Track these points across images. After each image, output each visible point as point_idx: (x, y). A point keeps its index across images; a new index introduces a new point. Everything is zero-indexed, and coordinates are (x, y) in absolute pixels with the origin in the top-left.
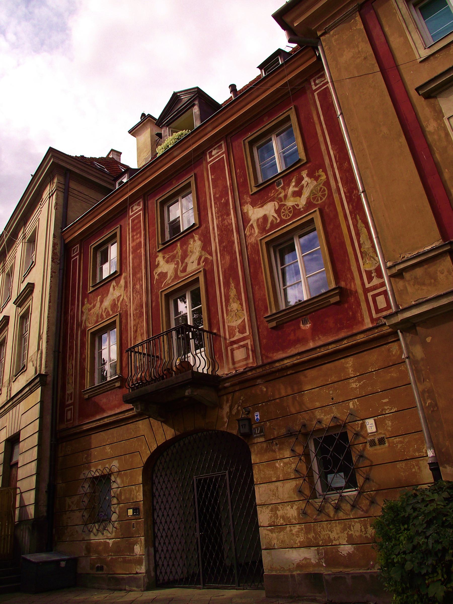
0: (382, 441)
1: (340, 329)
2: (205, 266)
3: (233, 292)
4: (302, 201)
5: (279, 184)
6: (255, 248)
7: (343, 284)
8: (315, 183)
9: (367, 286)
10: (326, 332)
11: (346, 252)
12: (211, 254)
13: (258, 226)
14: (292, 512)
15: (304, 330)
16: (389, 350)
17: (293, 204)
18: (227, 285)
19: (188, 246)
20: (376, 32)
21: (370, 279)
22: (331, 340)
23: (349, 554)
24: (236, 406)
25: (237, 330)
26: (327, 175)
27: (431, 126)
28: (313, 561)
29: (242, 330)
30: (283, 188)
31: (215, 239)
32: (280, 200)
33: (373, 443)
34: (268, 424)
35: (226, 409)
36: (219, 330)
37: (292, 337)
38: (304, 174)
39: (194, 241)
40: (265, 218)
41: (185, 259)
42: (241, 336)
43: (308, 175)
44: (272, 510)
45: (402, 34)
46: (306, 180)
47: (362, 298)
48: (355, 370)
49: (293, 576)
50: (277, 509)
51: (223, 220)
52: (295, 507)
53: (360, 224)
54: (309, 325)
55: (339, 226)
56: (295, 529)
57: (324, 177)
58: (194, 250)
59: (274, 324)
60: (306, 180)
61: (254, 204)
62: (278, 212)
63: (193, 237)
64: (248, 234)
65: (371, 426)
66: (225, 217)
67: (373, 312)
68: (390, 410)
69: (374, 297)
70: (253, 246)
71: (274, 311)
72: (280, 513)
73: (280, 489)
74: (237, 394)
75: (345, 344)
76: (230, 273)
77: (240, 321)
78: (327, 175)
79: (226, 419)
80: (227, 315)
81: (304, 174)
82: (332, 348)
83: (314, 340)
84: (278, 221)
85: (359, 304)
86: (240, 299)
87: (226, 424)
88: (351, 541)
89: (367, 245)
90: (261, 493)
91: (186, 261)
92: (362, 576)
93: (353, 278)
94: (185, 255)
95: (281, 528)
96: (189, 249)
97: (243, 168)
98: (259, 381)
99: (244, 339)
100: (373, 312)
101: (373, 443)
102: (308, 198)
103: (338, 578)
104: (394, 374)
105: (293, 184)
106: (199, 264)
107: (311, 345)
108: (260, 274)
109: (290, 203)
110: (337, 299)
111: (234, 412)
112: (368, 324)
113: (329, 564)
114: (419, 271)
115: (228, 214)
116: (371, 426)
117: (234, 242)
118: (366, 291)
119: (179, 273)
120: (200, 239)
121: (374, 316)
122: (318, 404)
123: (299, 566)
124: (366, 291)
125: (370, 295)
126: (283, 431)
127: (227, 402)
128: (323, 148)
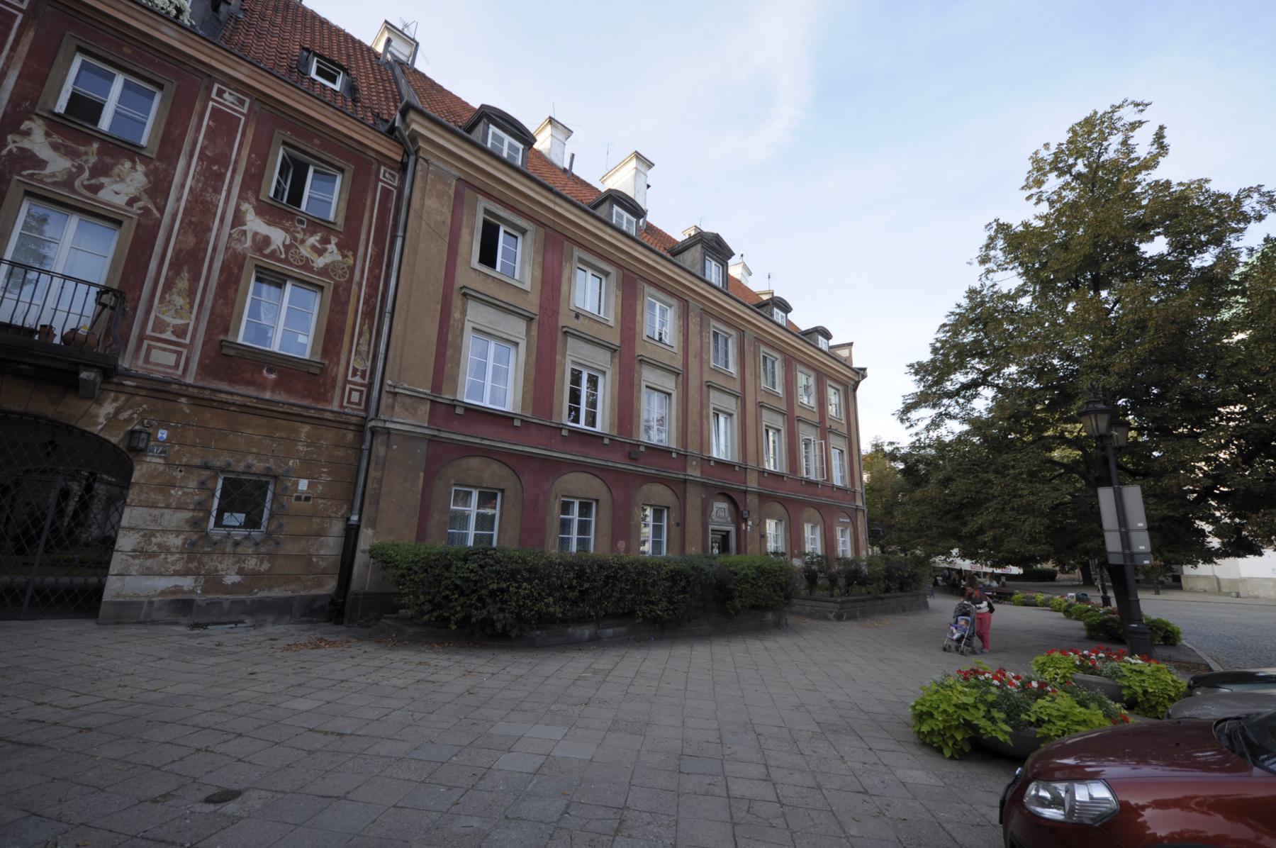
2: (139, 215)
3: (183, 284)
4: (320, 262)
5: (301, 222)
7: (326, 362)
8: (340, 258)
10: (289, 391)
11: (341, 340)
12: (162, 211)
13: (254, 240)
14: (174, 541)
15: (266, 379)
16: (345, 435)
18: (176, 266)
19: (115, 164)
21: (354, 375)
22: (292, 401)
23: (234, 584)
24: (130, 412)
25: (170, 329)
26: (355, 261)
27: (457, 315)
28: (186, 589)
29: (180, 332)
31: (179, 199)
32: (295, 239)
33: (298, 498)
34: (177, 447)
35: (108, 408)
36: (135, 309)
38: (334, 240)
39: (134, 168)
41: (101, 175)
42: (174, 338)
43: (336, 244)
44: (144, 536)
46: (332, 247)
48: (307, 437)
49: (151, 603)
50: (154, 535)
51: (204, 189)
52: (182, 537)
53: (366, 327)
54: (273, 376)
55: (345, 314)
56: (171, 559)
58: (128, 180)
60: (332, 247)
63: (134, 162)
64: (235, 236)
65: (303, 485)
66: (210, 190)
68: (325, 478)
69: (351, 390)
70: (235, 254)
73: (167, 517)
74: (138, 398)
75: (312, 413)
76: (189, 260)
77: (179, 322)
79: (102, 420)
80: (162, 299)
81: (334, 240)
82: (295, 410)
83: (273, 391)
84: (283, 256)
85: (334, 387)
86: (191, 294)
87: (100, 427)
88: (240, 572)
89: (364, 348)
90: (129, 516)
91: (102, 180)
92: (243, 602)
93: (338, 364)
94: (101, 170)
95: (153, 555)
96: (116, 170)
98: (183, 400)
102: (327, 266)
103: (212, 604)
106: (131, 202)
107: (268, 395)
108: (232, 290)
109: (305, 251)
110: (318, 371)
111: (125, 415)
112: (336, 409)
113: (204, 591)
114: (408, 401)
115: (217, 191)
116: (303, 485)
117: (210, 230)
118: (346, 382)
119: (77, 183)
120: (146, 175)
122: (254, 450)
123: (163, 593)
124: (346, 382)
125: (348, 386)
126: (197, 461)
127: (115, 400)
128: (363, 237)
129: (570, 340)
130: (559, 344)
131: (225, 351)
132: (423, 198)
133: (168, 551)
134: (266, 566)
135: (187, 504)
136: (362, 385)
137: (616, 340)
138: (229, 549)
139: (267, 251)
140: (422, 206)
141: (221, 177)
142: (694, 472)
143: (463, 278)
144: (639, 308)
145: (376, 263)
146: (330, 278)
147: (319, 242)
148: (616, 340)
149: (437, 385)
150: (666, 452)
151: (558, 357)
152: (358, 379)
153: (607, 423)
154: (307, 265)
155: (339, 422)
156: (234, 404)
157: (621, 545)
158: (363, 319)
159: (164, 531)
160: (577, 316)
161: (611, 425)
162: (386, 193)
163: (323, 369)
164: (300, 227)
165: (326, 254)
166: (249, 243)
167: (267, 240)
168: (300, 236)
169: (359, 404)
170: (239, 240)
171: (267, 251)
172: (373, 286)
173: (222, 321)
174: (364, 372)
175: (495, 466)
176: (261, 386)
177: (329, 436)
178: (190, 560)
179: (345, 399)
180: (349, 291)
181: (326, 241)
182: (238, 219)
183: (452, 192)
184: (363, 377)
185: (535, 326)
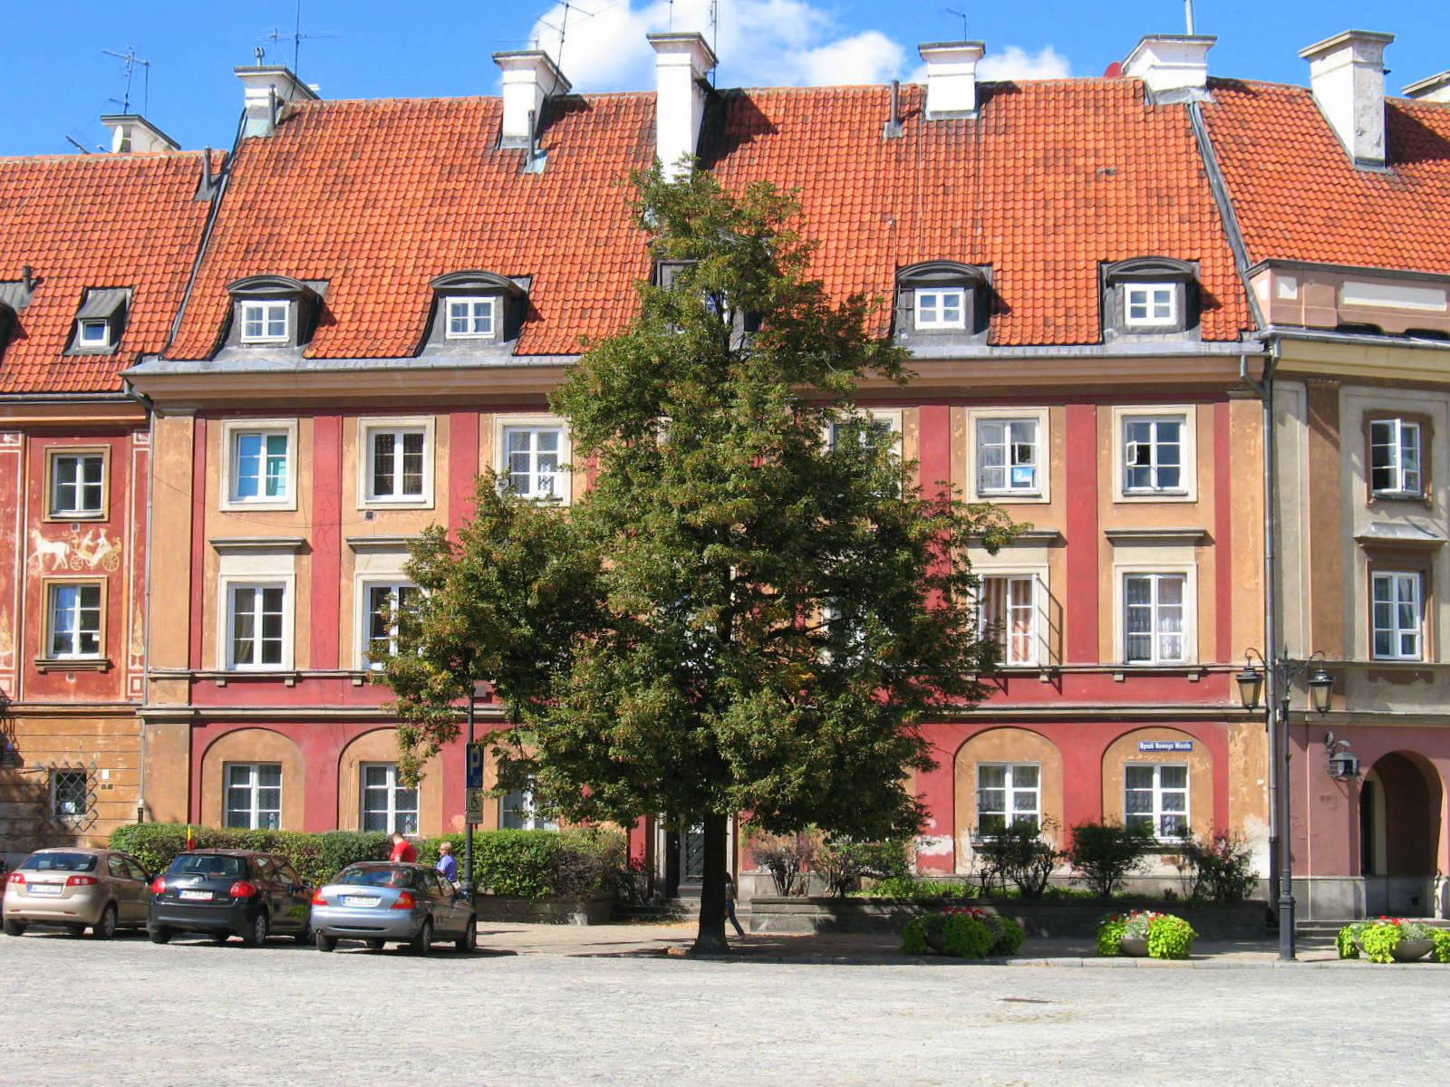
0: (110, 787)
1: (98, 694)
4: (94, 560)
5: (75, 528)
6: (36, 583)
11: (120, 631)
20: (200, 451)
21: (133, 663)
27: (209, 574)
30: (78, 534)
33: (104, 787)
37: (56, 685)
38: (103, 532)
40: (53, 557)
42: (6, 668)
45: (217, 472)
46: (103, 540)
47: (123, 675)
53: (138, 612)
54: (73, 681)
55: (120, 603)
56: (28, 839)
57: (119, 547)
59: (42, 668)
61: (44, 534)
62: (68, 557)
65: (105, 774)
69: (133, 678)
71: (44, 658)
72: (17, 826)
75: (102, 709)
77: (7, 653)
81: (103, 532)
85: (119, 679)
95: (18, 837)
97: (39, 481)
99: (8, 672)
101: (104, 787)
102: (100, 561)
104: (131, 741)
107: (72, 700)
109: (82, 555)
110: (103, 668)
112: (122, 699)
114: (167, 683)
115: (13, 531)
116: (105, 774)
117: (13, 567)
118: (128, 671)
124: (128, 671)
125: (130, 675)
128: (127, 516)
129: (361, 558)
132: (161, 458)
133: (23, 833)
139: (54, 568)
141: (13, 516)
143: (216, 529)
146: (105, 572)
151: (344, 582)
152: (137, 667)
158: (135, 604)
159: (23, 819)
164: (75, 532)
165: (99, 550)
166: (41, 565)
167: (53, 557)
168: (75, 542)
169: (141, 691)
170: (34, 567)
171: (54, 568)
172: (140, 567)
175: (268, 736)
176: (64, 691)
177: (120, 725)
180: (121, 578)
181: (97, 536)
182: (32, 549)
184: (141, 663)
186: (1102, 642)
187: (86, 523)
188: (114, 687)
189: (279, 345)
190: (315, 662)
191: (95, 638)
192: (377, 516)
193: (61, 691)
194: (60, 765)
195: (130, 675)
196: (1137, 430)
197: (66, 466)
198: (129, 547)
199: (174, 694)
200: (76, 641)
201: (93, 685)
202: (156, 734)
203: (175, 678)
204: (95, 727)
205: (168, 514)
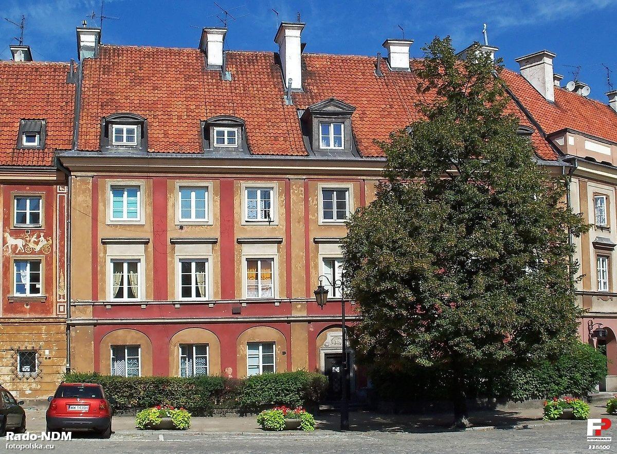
0: (50, 358)
4: (38, 248)
9: (58, 300)
10: (35, 312)
17: (33, 247)
21: (60, 298)
22: (37, 316)
26: (52, 241)
27: (101, 255)
32: (26, 241)
33: (46, 358)
37: (19, 309)
38: (42, 234)
46: (42, 238)
47: (55, 304)
54: (28, 307)
60: (42, 238)
61: (11, 235)
67: (58, 311)
75: (45, 320)
78: (52, 241)
81: (42, 234)
84: (23, 251)
100: (58, 311)
101: (46, 358)
105: (35, 237)
107: (28, 316)
109: (31, 245)
116: (47, 352)
118: (57, 302)
121: (58, 313)
124: (57, 302)
125: (58, 304)
126: (9, 348)
130: (169, 250)
131: (10, 301)
132: (76, 198)
134: (39, 386)
135: (9, 364)
136: (64, 302)
137: (217, 235)
138: (25, 380)
139: (17, 252)
140: (76, 202)
142: (299, 313)
144: (236, 202)
145: (62, 239)
146: (43, 254)
147: (36, 238)
148: (217, 235)
149: (95, 296)
150: (269, 303)
151: (169, 259)
153: (212, 293)
154: (33, 252)
155: (57, 322)
156: (16, 323)
157: (229, 371)
158: (60, 270)
160: (181, 228)
161: (215, 294)
162: (62, 198)
163: (46, 298)
165: (40, 243)
166: (10, 250)
171: (17, 252)
172: (62, 252)
173: (6, 290)
174: (64, 296)
175: (133, 333)
177: (54, 329)
178: (14, 385)
179: (58, 311)
181: (39, 237)
183: (90, 187)
185: (151, 245)
186: (151, 283)
187: (33, 232)
188: (49, 310)
189: (132, 147)
190: (156, 298)
191: (37, 286)
192: (185, 228)
193: (22, 312)
194: (23, 348)
195: (58, 304)
196: (327, 193)
197: (21, 200)
198: (56, 242)
199: (84, 312)
200: (28, 287)
201: (39, 309)
202: (76, 332)
203: (86, 305)
204: (41, 329)
205: (81, 227)
